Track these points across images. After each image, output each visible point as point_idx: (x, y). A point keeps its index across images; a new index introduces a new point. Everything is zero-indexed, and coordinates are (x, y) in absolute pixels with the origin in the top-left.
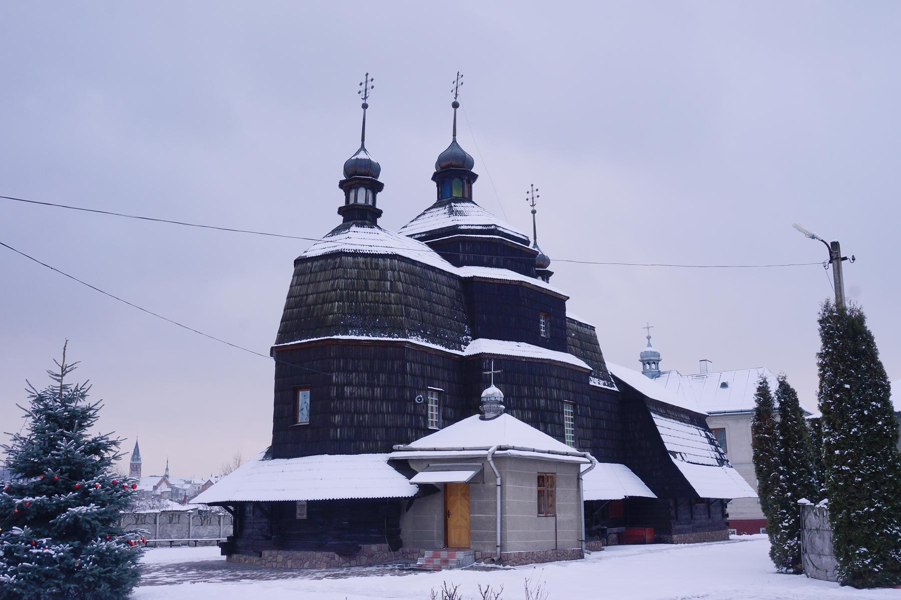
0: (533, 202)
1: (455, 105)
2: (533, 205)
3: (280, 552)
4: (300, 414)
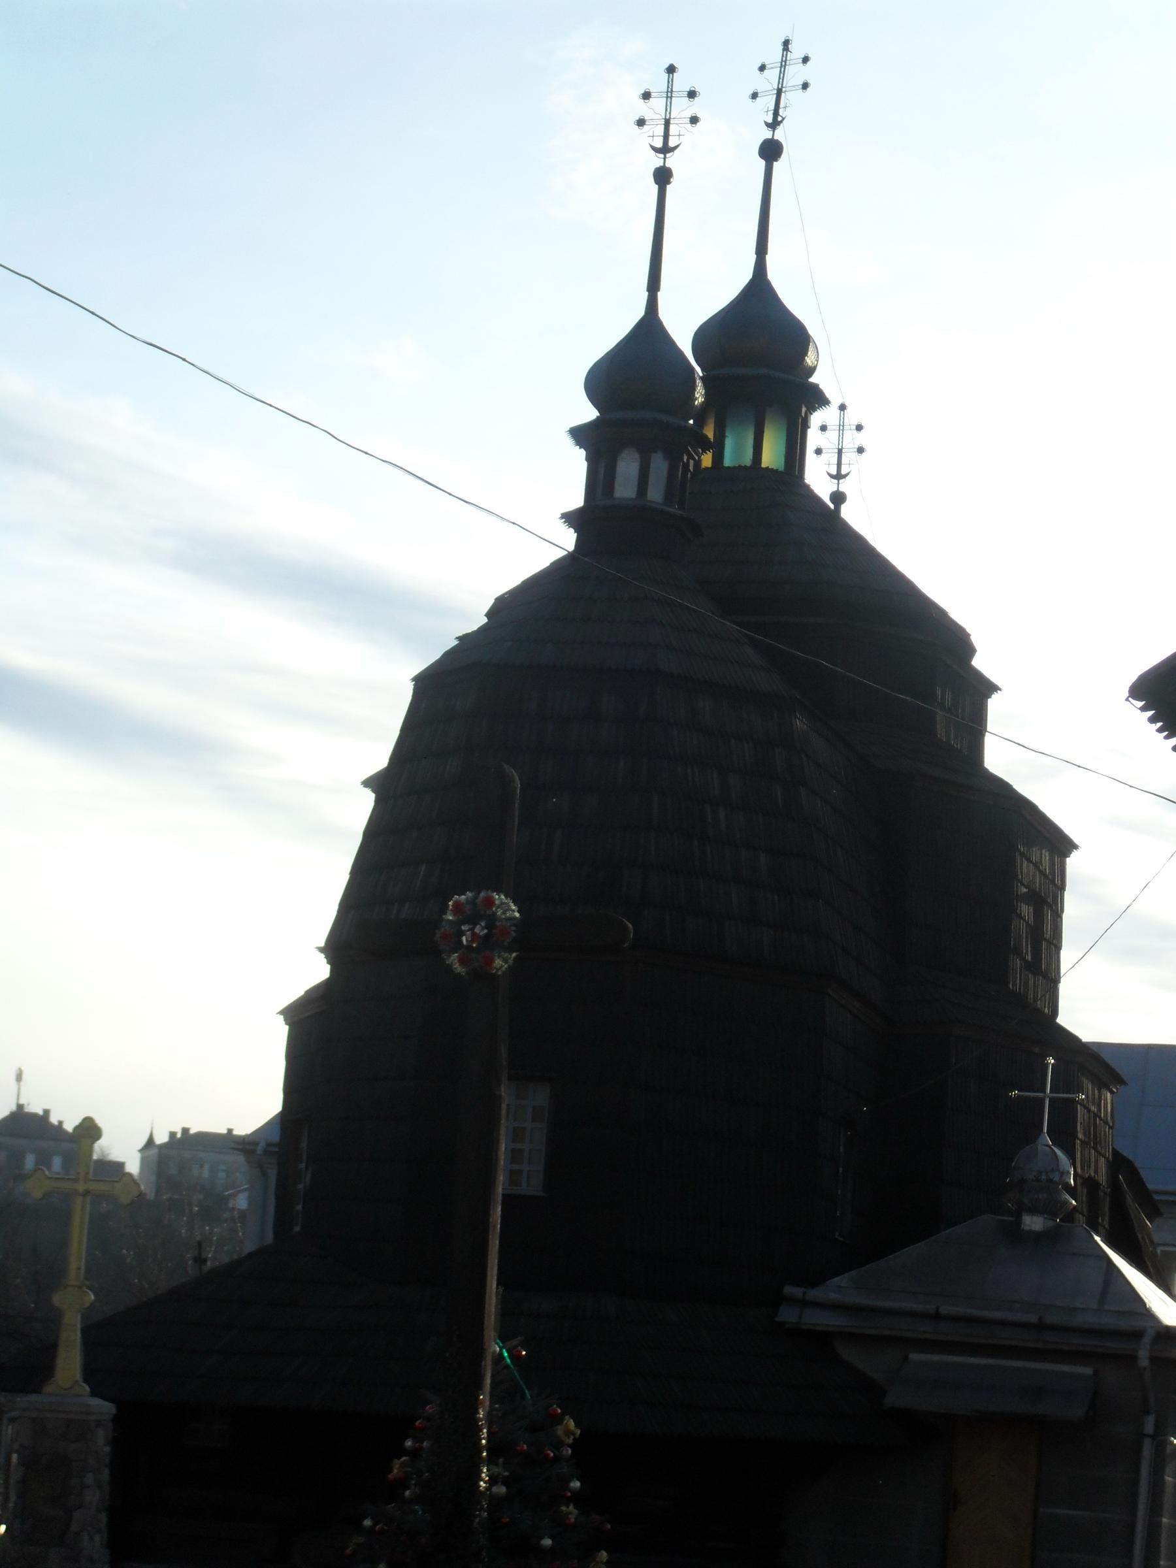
1: (771, 151)
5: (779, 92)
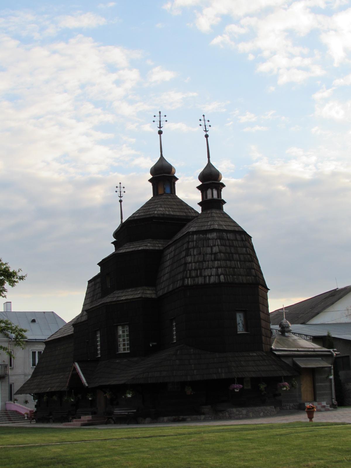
0: (120, 194)
1: (160, 133)
2: (121, 197)
4: (238, 327)
5: (160, 122)
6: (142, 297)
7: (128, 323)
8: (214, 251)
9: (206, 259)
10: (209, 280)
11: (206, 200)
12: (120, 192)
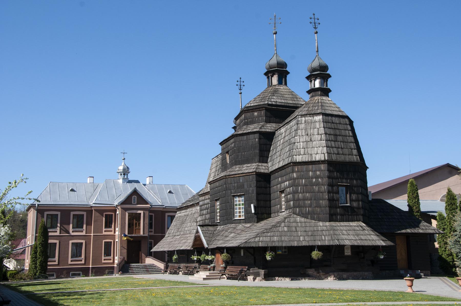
3: (344, 273)
5: (275, 23)
6: (256, 172)
7: (243, 193)
8: (320, 133)
9: (313, 139)
10: (315, 158)
11: (314, 88)
12: (240, 85)
